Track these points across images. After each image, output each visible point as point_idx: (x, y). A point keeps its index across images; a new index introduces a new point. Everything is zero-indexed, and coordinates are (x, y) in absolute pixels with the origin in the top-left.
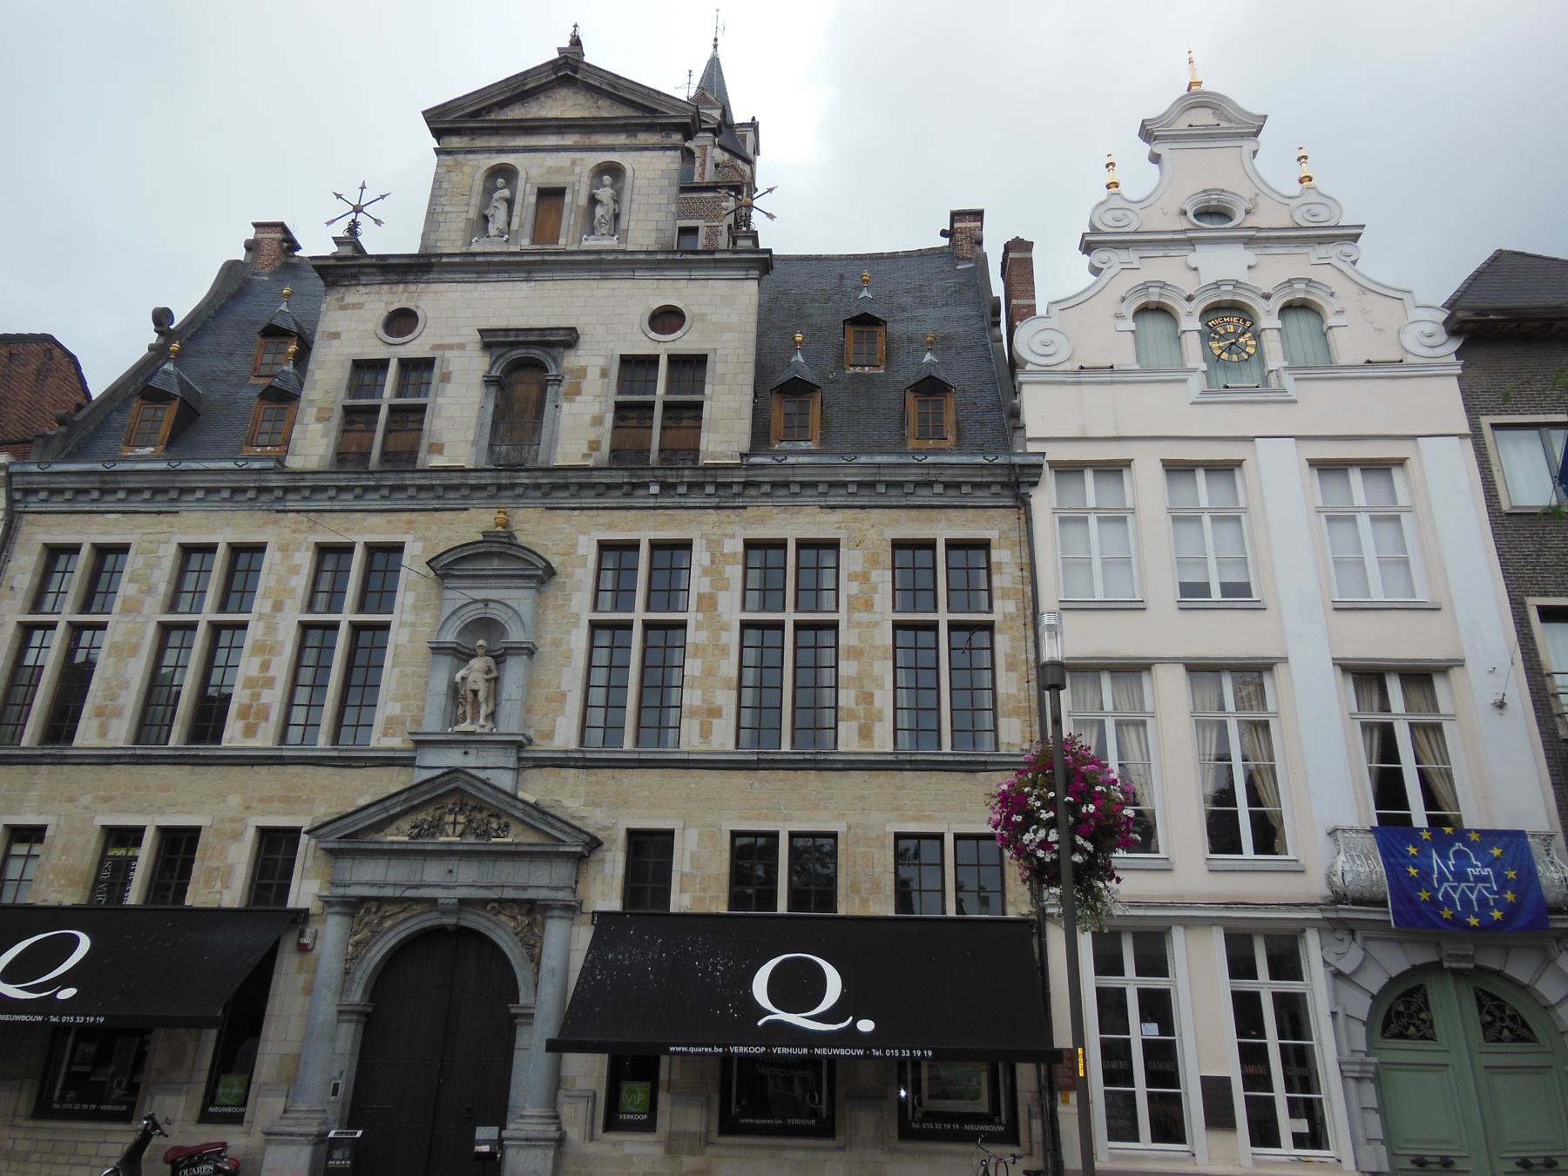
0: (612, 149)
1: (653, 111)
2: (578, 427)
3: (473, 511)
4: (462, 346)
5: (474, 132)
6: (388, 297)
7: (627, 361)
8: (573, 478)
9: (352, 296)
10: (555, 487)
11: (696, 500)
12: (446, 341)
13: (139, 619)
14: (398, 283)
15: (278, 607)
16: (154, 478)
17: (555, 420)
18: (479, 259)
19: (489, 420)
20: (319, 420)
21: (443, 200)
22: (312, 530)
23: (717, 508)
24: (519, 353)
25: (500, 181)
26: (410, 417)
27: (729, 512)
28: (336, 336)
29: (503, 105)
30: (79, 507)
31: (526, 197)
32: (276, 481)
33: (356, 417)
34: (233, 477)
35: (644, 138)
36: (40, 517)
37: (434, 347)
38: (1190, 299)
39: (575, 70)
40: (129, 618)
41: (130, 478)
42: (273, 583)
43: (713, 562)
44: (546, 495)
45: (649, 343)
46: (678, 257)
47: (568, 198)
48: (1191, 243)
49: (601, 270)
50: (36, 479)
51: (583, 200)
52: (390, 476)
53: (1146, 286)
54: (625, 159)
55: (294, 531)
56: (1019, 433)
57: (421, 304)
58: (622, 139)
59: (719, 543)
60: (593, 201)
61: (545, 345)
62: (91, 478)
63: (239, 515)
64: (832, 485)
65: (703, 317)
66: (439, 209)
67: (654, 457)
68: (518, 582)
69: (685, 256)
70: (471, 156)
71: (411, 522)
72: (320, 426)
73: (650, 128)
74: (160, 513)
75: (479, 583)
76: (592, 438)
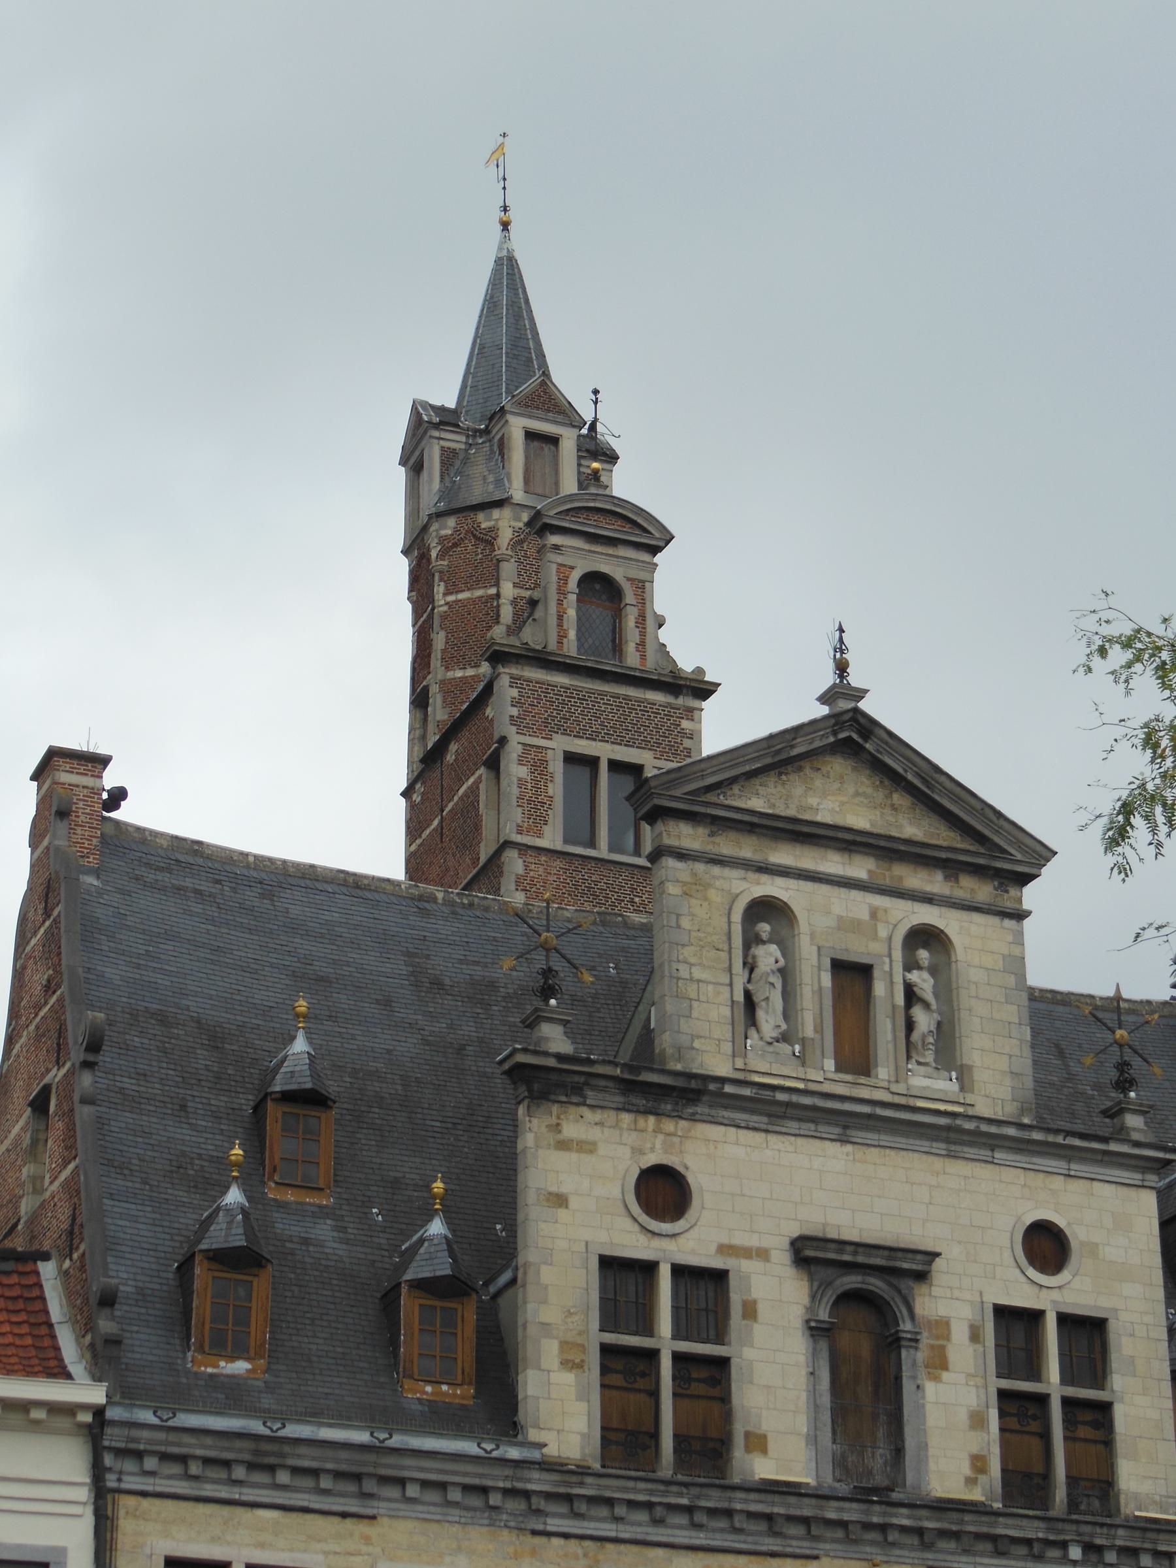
0: (928, 899)
1: (981, 839)
3: (825, 1561)
4: (763, 1254)
5: (719, 823)
6: (631, 1138)
7: (1002, 1313)
8: (972, 1525)
9: (579, 1124)
10: (943, 1534)
14: (647, 1112)
16: (344, 1454)
17: (920, 1408)
18: (781, 1097)
19: (826, 1400)
20: (568, 1364)
24: (852, 1281)
25: (764, 928)
26: (709, 1377)
28: (560, 1200)
30: (209, 1490)
31: (815, 980)
32: (538, 1482)
33: (625, 1368)
34: (469, 1468)
36: (145, 1503)
37: (725, 1249)
41: (303, 1450)
44: (926, 1546)
46: (1060, 1139)
49: (948, 1141)
50: (145, 1434)
51: (900, 1000)
52: (714, 1493)
58: (935, 883)
61: (890, 1272)
62: (238, 1444)
65: (1092, 1249)
70: (716, 870)
72: (569, 1378)
73: (978, 871)
74: (344, 1515)
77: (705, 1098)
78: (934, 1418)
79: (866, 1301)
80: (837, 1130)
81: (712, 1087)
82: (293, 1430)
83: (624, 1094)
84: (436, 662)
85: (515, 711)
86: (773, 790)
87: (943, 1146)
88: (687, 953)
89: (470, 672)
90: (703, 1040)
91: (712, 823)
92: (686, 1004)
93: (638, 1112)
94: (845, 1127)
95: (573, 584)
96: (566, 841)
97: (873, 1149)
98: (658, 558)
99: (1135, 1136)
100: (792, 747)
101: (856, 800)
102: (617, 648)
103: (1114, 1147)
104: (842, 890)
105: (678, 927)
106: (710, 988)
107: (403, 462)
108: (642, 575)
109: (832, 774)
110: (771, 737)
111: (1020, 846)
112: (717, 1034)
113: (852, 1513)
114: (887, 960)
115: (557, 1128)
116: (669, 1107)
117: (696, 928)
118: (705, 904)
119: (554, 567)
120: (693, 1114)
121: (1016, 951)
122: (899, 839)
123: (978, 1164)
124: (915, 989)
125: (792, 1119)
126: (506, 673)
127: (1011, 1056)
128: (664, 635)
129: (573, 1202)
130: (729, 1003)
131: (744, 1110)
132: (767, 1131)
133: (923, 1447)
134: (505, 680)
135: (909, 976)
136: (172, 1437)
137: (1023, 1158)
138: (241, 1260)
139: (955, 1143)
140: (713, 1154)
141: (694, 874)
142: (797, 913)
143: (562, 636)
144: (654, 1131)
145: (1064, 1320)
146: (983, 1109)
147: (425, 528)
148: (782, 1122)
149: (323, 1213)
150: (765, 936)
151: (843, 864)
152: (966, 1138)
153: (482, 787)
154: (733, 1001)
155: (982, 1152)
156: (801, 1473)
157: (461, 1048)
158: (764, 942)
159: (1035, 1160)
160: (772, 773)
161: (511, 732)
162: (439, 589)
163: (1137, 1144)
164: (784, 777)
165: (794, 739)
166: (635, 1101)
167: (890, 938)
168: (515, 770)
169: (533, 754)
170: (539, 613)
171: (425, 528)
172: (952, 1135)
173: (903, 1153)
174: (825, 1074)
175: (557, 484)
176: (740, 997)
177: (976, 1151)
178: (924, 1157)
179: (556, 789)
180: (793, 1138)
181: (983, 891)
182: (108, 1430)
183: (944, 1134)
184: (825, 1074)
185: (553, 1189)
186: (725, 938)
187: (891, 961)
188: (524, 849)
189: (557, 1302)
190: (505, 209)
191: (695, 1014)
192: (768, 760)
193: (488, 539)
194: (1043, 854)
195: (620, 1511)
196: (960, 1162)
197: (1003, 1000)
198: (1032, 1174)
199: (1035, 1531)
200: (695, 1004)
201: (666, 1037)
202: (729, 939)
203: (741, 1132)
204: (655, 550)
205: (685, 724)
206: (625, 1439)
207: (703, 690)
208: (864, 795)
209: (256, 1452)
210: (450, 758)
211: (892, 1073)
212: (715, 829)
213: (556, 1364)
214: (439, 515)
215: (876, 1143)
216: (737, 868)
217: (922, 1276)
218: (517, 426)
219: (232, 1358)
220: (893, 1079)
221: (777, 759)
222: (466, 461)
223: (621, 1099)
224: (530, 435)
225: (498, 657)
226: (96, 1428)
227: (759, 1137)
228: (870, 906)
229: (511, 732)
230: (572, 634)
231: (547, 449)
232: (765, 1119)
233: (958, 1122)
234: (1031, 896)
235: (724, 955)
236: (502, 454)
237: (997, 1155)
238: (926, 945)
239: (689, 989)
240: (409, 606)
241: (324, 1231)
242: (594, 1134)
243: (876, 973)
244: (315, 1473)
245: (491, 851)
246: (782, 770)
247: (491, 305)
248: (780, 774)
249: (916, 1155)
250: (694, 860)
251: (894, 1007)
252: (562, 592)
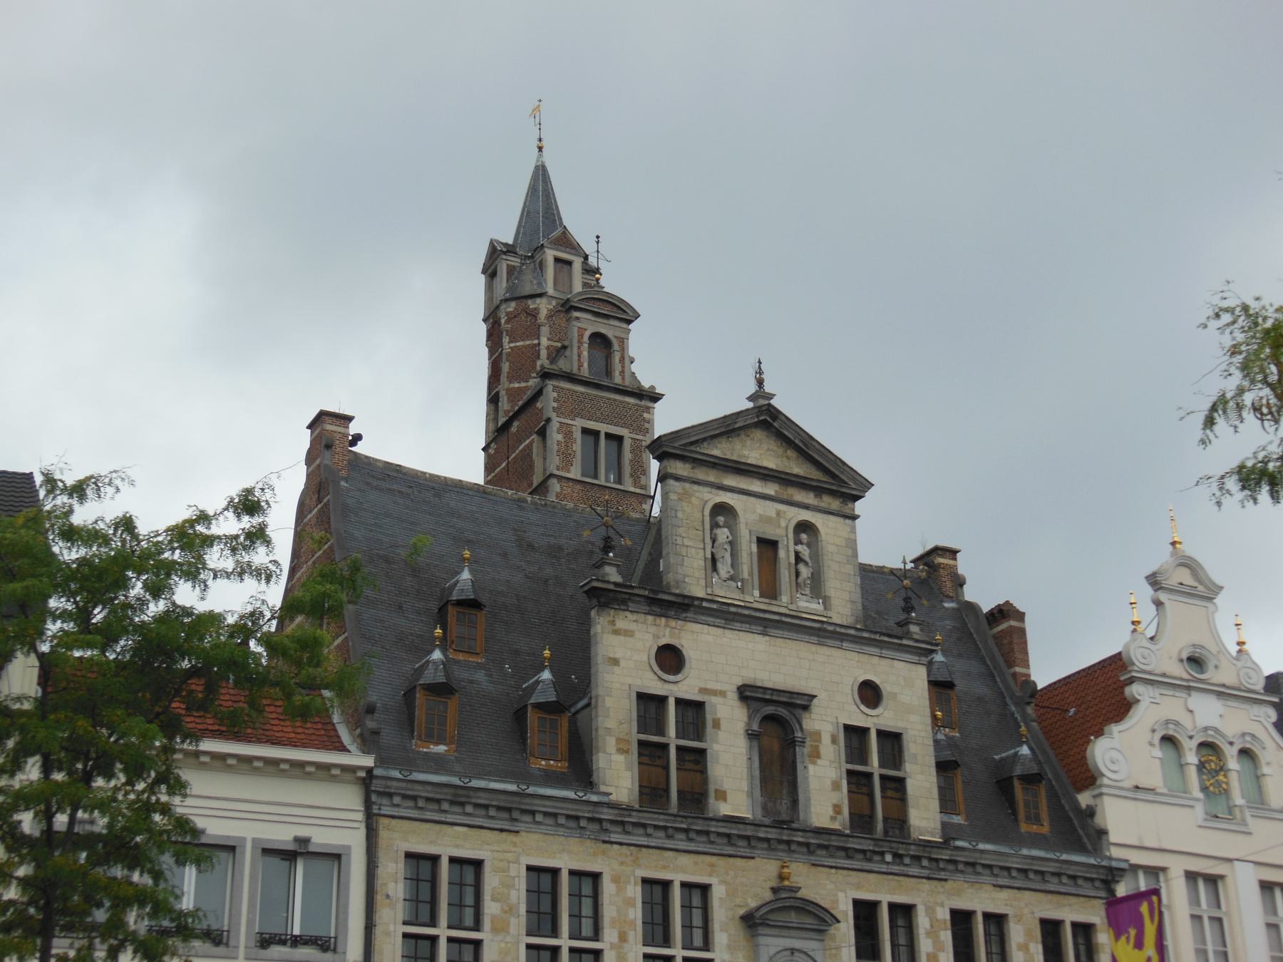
0: (806, 507)
2: (823, 792)
3: (758, 860)
4: (722, 694)
6: (652, 629)
7: (849, 729)
9: (625, 621)
10: (820, 846)
11: (915, 870)
12: (711, 686)
13: (509, 939)
14: (661, 616)
15: (623, 938)
16: (502, 797)
18: (733, 609)
19: (757, 773)
20: (620, 751)
22: (636, 862)
23: (929, 878)
24: (770, 709)
25: (721, 519)
26: (695, 759)
27: (935, 883)
28: (615, 662)
30: (428, 815)
31: (749, 549)
32: (606, 814)
33: (651, 753)
34: (570, 806)
36: (394, 822)
37: (703, 691)
38: (1191, 737)
40: (500, 937)
41: (481, 794)
42: (615, 914)
43: (932, 926)
44: (811, 853)
45: (861, 715)
46: (877, 637)
47: (782, 553)
48: (1189, 688)
49: (818, 636)
50: (395, 784)
51: (793, 560)
52: (700, 822)
53: (1167, 722)
55: (622, 863)
56: (1104, 838)
57: (684, 642)
58: (809, 498)
59: (934, 912)
60: (798, 558)
62: (446, 790)
63: (572, 841)
64: (1002, 868)
67: (880, 826)
68: (813, 935)
70: (696, 487)
71: (712, 865)
72: (621, 758)
73: (833, 493)
74: (502, 830)
75: (784, 932)
76: (835, 802)
78: (813, 784)
79: (777, 720)
81: (696, 603)
82: (476, 783)
84: (504, 378)
85: (555, 405)
88: (681, 530)
89: (523, 385)
95: (586, 339)
96: (583, 475)
98: (631, 327)
99: (916, 637)
102: (609, 373)
103: (905, 642)
107: (484, 272)
108: (623, 335)
111: (854, 480)
112: (697, 574)
113: (772, 834)
115: (613, 623)
119: (576, 329)
121: (852, 536)
126: (550, 384)
128: (634, 368)
129: (622, 663)
131: (712, 616)
133: (808, 799)
134: (550, 388)
136: (410, 786)
138: (442, 690)
140: (697, 640)
143: (580, 366)
145: (880, 733)
146: (836, 620)
147: (498, 307)
149: (479, 666)
153: (535, 445)
156: (745, 813)
157: (546, 581)
161: (553, 415)
162: (506, 340)
163: (917, 641)
167: (787, 528)
168: (555, 436)
169: (565, 427)
170: (568, 353)
171: (498, 307)
174: (753, 597)
175: (571, 286)
176: (709, 556)
179: (577, 447)
181: (835, 504)
182: (374, 781)
184: (753, 597)
185: (612, 656)
188: (560, 478)
189: (614, 717)
190: (540, 140)
193: (534, 314)
194: (866, 485)
195: (650, 831)
199: (867, 845)
201: (670, 575)
204: (629, 322)
205: (645, 415)
206: (652, 792)
207: (656, 398)
209: (455, 795)
210: (514, 429)
213: (614, 750)
214: (506, 300)
217: (806, 708)
218: (550, 254)
219: (437, 744)
222: (521, 272)
224: (557, 260)
225: (546, 375)
226: (367, 780)
227: (720, 631)
229: (553, 415)
230: (586, 365)
231: (566, 267)
234: (859, 507)
236: (541, 269)
238: (804, 532)
240: (487, 350)
241: (480, 676)
242: (633, 626)
243: (780, 545)
244: (486, 807)
245: (541, 479)
247: (532, 190)
252: (580, 343)
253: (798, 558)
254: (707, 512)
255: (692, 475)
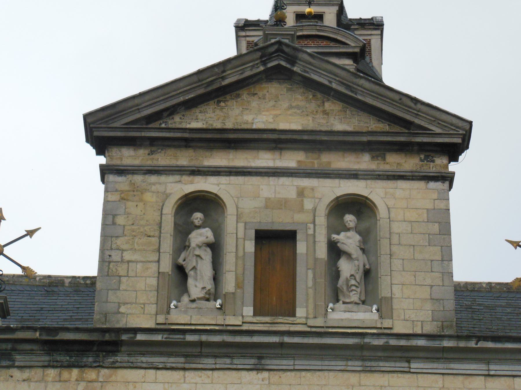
0: (354, 175)
5: (155, 143)
14: (70, 366)
18: (190, 338)
21: (120, 242)
29: (191, 104)
35: (395, 161)
39: (293, 61)
46: (472, 344)
47: (301, 247)
49: (363, 359)
51: (322, 252)
54: (374, 191)
58: (364, 162)
60: (335, 251)
66: (116, 256)
69: (482, 344)
70: (153, 178)
73: (403, 148)
77: (123, 349)
80: (253, 361)
81: (124, 337)
83: (49, 354)
86: (212, 115)
87: (359, 363)
90: (129, 306)
91: (151, 145)
92: (115, 280)
93: (62, 367)
94: (260, 358)
97: (289, 373)
100: (223, 78)
101: (290, 112)
104: (271, 179)
105: (114, 223)
106: (139, 266)
109: (267, 95)
110: (200, 72)
112: (142, 299)
114: (312, 226)
116: (91, 359)
117: (130, 223)
118: (141, 205)
120: (114, 363)
122: (321, 131)
123: (395, 375)
124: (339, 245)
125: (207, 356)
127: (432, 286)
130: (156, 275)
131: (161, 354)
132: (184, 369)
135: (335, 237)
137: (441, 366)
139: (370, 360)
141: (132, 184)
142: (225, 201)
144: (77, 380)
146: (399, 329)
148: (198, 360)
150: (197, 222)
151: (274, 160)
152: (380, 354)
154: (159, 273)
155: (398, 364)
158: (198, 227)
159: (452, 366)
160: (212, 102)
164: (222, 104)
165: (224, 71)
166: (58, 358)
167: (315, 210)
172: (366, 353)
173: (318, 373)
177: (393, 364)
178: (340, 374)
180: (210, 372)
181: (410, 163)
183: (358, 353)
186: (156, 227)
187: (315, 225)
191: (122, 287)
192: (201, 91)
196: (376, 375)
197: (427, 244)
198: (451, 377)
200: (124, 279)
202: (160, 227)
203: (159, 372)
208: (298, 107)
211: (311, 311)
212: (154, 149)
215: (291, 368)
216: (172, 174)
220: (311, 316)
221: (210, 89)
223: (47, 358)
227: (177, 375)
228: (297, 187)
232: (182, 360)
233: (367, 340)
235: (155, 240)
237: (413, 365)
239: (119, 269)
243: (298, 237)
246: (221, 99)
248: (219, 102)
249: (331, 374)
250: (133, 174)
251: (316, 260)
253: (335, 251)
254: (169, 209)
255: (149, 163)
